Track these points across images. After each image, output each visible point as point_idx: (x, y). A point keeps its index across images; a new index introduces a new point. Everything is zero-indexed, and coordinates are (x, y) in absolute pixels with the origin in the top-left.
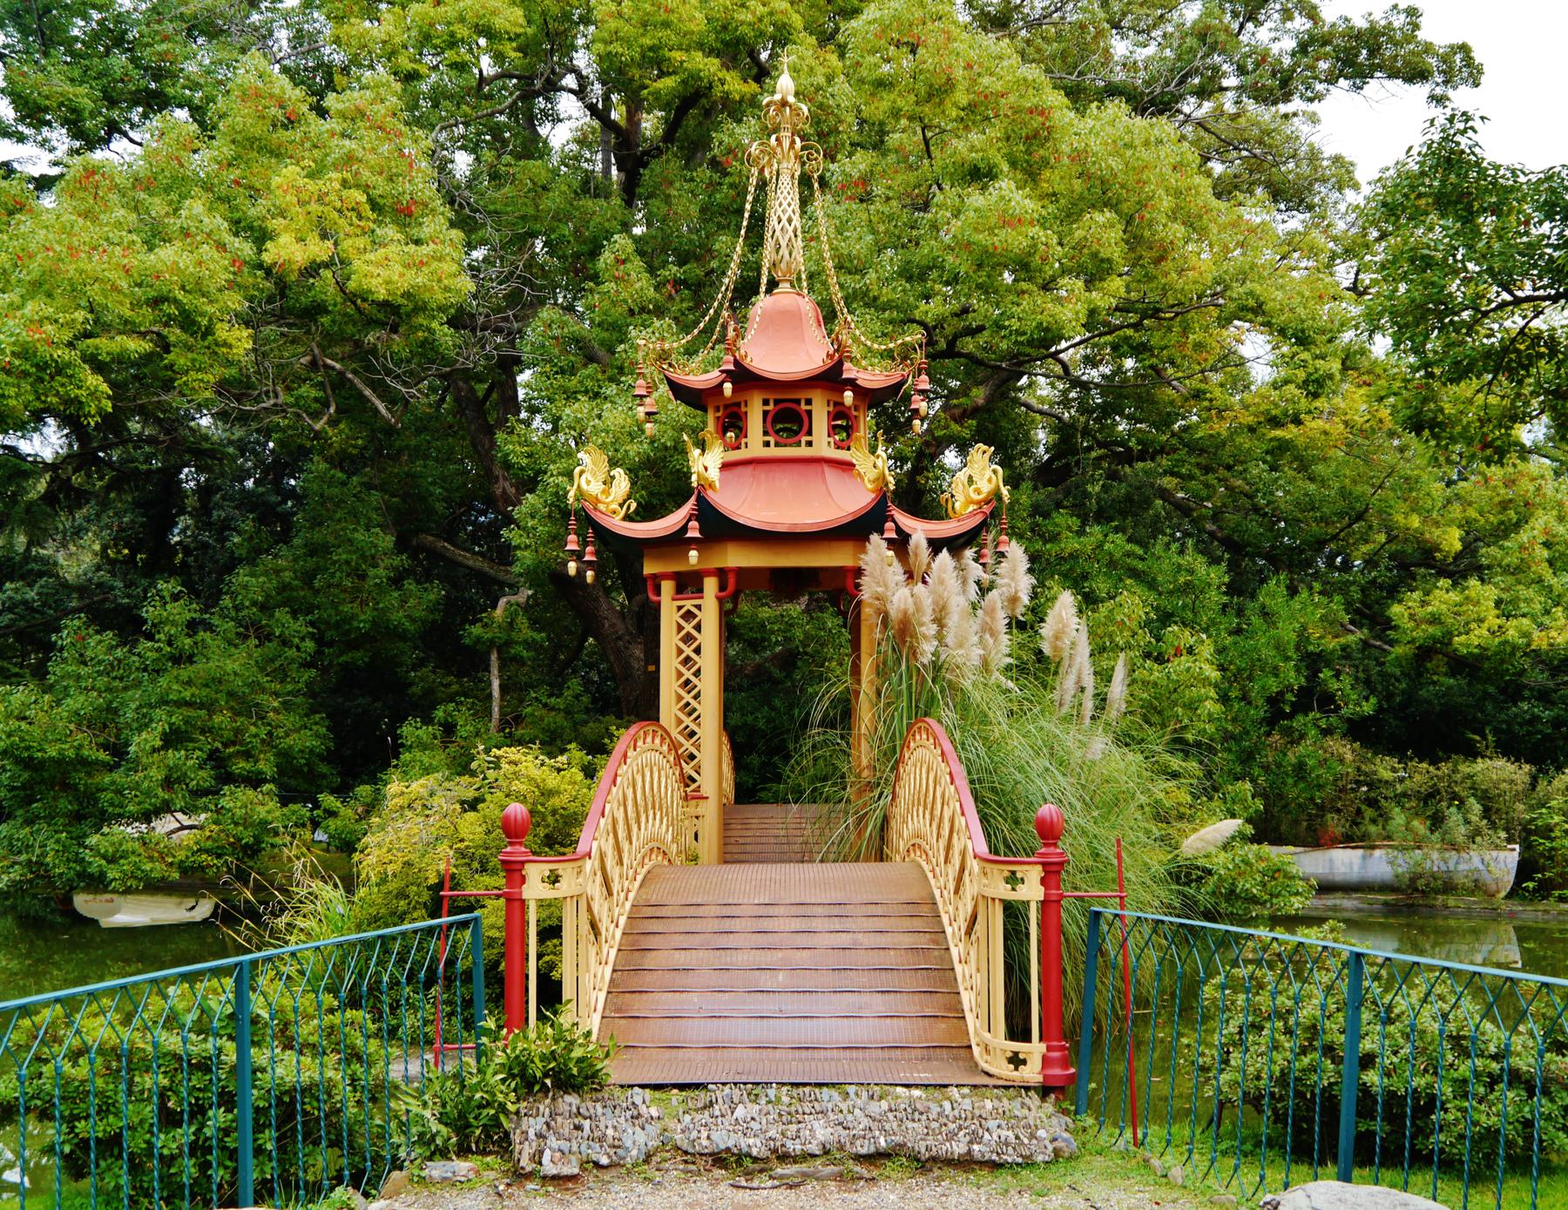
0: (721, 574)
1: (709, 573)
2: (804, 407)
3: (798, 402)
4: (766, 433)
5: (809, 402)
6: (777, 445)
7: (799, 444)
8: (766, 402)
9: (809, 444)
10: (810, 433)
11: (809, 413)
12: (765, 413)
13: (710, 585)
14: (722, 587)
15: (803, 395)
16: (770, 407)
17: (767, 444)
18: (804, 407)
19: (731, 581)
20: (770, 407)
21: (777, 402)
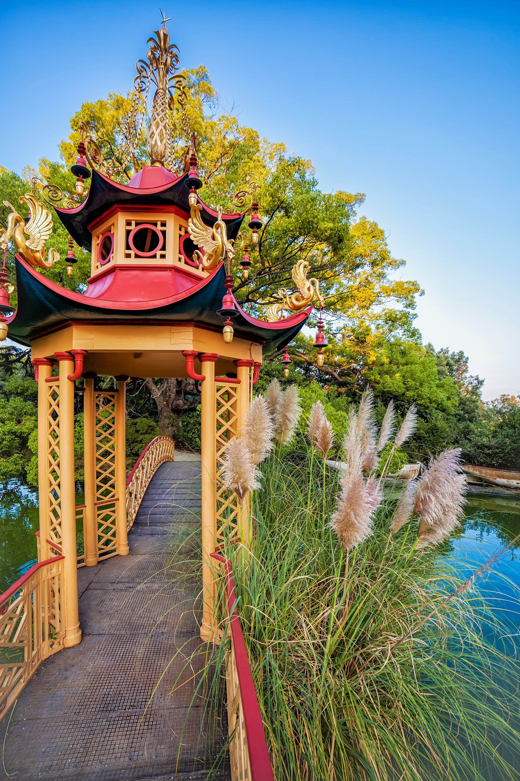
2: (159, 228)
4: (128, 247)
5: (164, 224)
6: (137, 256)
7: (154, 256)
8: (129, 223)
9: (163, 256)
10: (164, 248)
11: (164, 233)
12: (128, 232)
15: (158, 218)
16: (133, 227)
17: (128, 256)
18: (159, 228)
20: (133, 227)
21: (137, 224)
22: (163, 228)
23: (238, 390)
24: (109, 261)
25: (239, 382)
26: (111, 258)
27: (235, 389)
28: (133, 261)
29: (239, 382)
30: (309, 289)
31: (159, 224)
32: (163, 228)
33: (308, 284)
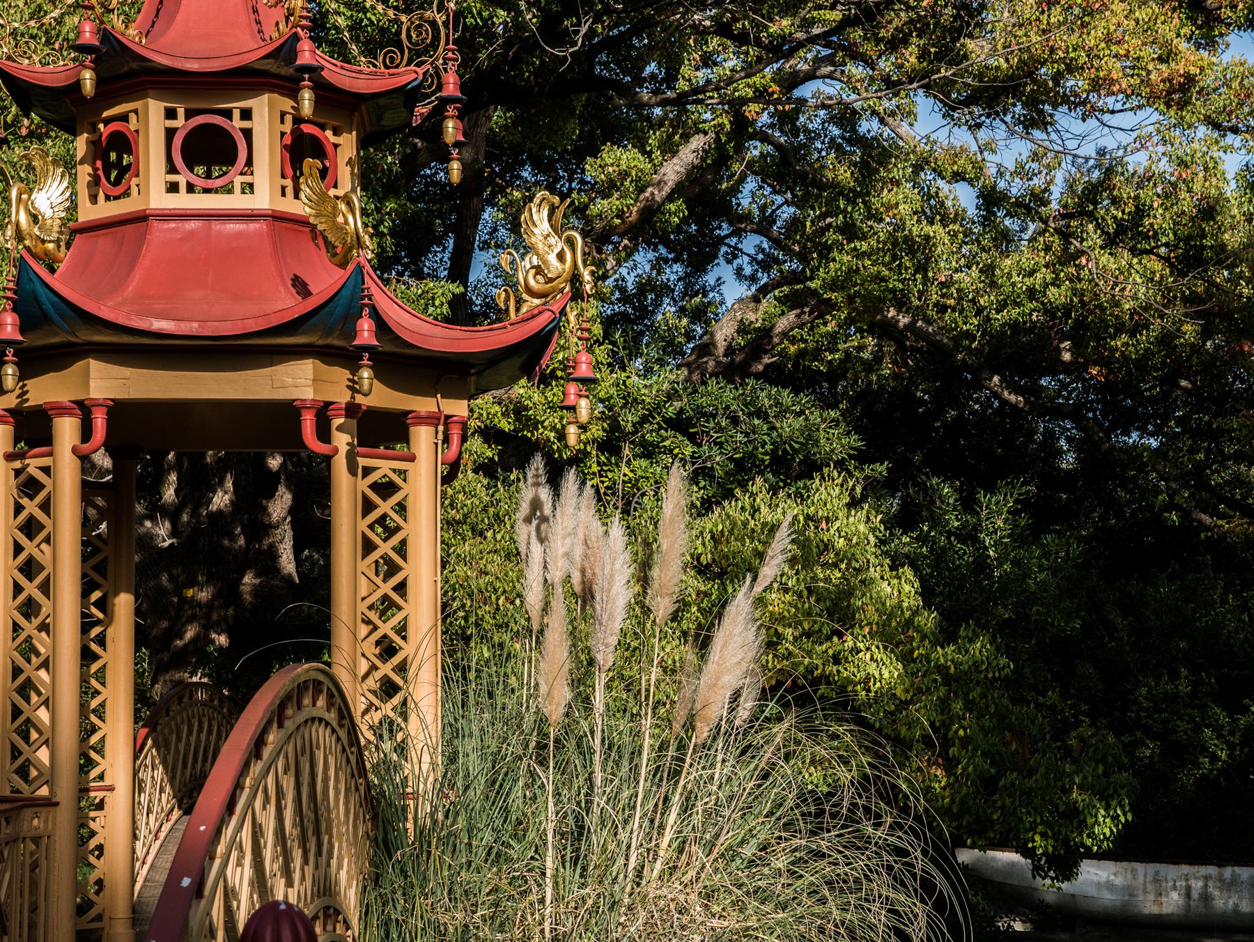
0: (84, 409)
1: (62, 410)
2: (237, 123)
3: (228, 114)
4: (172, 169)
5: (246, 114)
8: (171, 114)
11: (248, 133)
12: (170, 133)
13: (67, 430)
14: (86, 432)
16: (180, 122)
17: (173, 188)
18: (237, 123)
19: (99, 421)
20: (180, 122)
21: (189, 114)
22: (246, 124)
23: (410, 475)
24: (126, 193)
25: (412, 459)
26: (134, 190)
27: (402, 473)
28: (183, 201)
29: (412, 459)
30: (561, 257)
31: (236, 114)
32: (246, 124)
33: (558, 244)
